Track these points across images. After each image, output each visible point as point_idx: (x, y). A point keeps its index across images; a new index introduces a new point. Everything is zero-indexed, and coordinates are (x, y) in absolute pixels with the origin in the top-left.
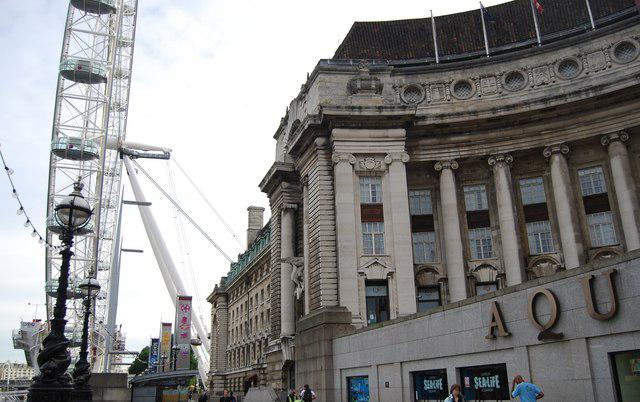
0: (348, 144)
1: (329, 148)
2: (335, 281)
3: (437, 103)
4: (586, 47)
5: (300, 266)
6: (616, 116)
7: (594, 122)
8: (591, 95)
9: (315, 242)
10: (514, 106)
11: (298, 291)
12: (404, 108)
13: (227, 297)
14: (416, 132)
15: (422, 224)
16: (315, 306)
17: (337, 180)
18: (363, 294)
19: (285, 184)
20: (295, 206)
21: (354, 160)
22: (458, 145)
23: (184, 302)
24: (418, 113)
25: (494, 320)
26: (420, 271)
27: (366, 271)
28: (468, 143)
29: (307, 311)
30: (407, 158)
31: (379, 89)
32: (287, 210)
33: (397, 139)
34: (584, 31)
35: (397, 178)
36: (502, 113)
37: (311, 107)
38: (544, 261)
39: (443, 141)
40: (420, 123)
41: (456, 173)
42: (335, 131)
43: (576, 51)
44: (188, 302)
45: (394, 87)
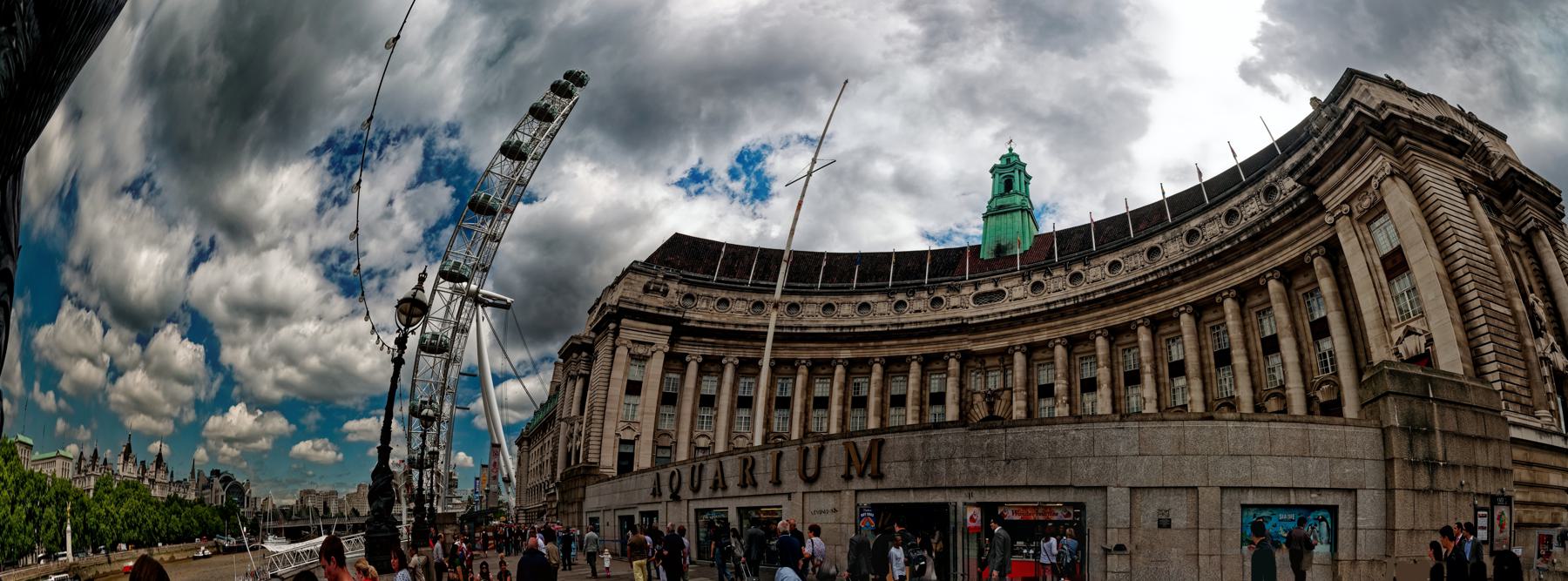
0: (632, 331)
1: (616, 333)
3: (702, 313)
6: (809, 349)
9: (592, 406)
14: (681, 330)
15: (669, 399)
16: (586, 458)
30: (667, 349)
31: (665, 293)
33: (665, 333)
35: (657, 364)
37: (612, 299)
41: (700, 365)
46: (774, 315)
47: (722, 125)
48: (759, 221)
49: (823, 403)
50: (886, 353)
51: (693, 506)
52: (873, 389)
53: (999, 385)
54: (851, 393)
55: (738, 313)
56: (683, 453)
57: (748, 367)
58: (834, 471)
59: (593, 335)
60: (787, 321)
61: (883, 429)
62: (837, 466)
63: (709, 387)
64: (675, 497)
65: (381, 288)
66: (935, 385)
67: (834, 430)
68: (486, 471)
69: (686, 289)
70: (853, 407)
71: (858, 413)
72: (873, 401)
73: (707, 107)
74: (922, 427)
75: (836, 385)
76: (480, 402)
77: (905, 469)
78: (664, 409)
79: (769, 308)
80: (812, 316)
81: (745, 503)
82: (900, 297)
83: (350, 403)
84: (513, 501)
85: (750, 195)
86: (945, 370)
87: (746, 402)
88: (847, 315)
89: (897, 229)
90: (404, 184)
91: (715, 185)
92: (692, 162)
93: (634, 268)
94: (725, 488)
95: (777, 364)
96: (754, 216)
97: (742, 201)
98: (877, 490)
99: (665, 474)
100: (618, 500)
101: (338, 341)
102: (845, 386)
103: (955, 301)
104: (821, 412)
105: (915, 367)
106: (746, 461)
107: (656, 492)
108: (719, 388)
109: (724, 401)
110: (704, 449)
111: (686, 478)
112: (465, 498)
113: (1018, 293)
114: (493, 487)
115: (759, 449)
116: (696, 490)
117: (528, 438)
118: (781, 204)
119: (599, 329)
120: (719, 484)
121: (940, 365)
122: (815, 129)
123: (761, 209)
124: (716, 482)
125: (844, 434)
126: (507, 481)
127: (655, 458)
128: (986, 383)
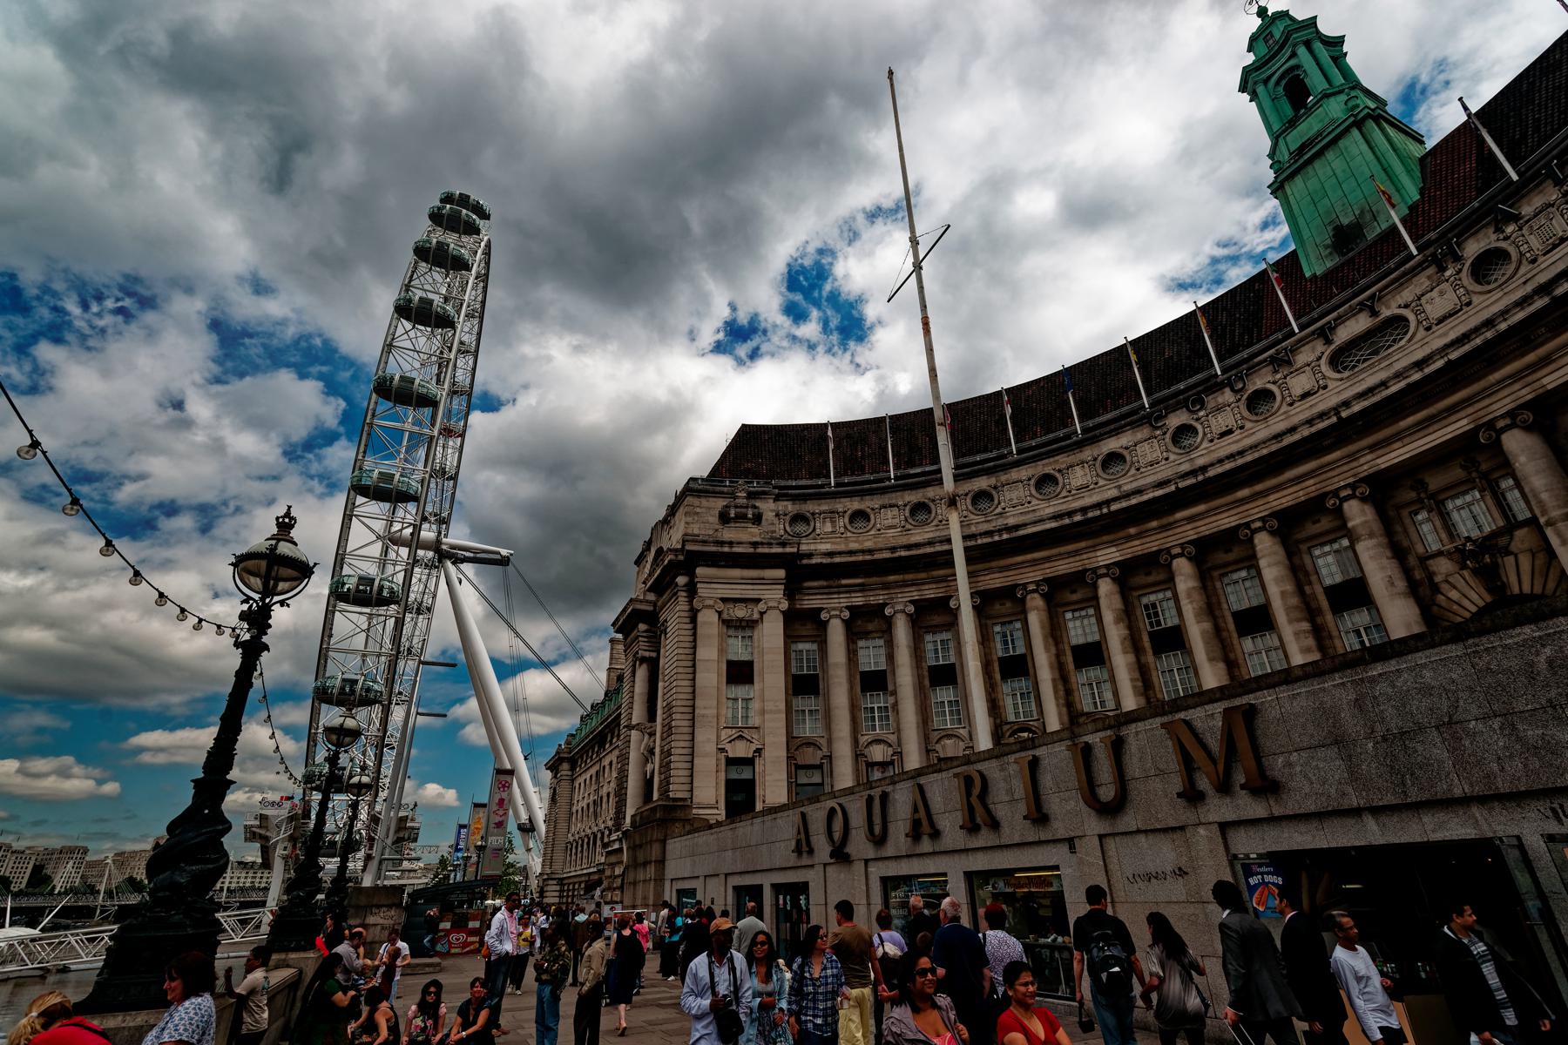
0: (715, 585)
1: (692, 590)
2: (688, 758)
3: (828, 538)
4: (1003, 478)
5: (652, 734)
6: (1035, 562)
7: (1007, 568)
8: (1005, 536)
9: (669, 708)
10: (917, 545)
11: (649, 767)
12: (783, 544)
13: (573, 764)
14: (799, 573)
15: (804, 685)
16: (665, 791)
17: (699, 631)
18: (722, 776)
19: (642, 627)
20: (654, 655)
21: (720, 607)
22: (850, 589)
23: (503, 778)
24: (803, 547)
25: (916, 810)
26: (795, 744)
27: (728, 747)
28: (863, 588)
29: (656, 796)
30: (785, 605)
31: (758, 519)
32: (643, 660)
33: (775, 582)
34: (1004, 456)
35: (772, 632)
36: (903, 553)
38: (949, 736)
39: (831, 583)
40: (805, 561)
41: (848, 624)
42: (700, 571)
43: (993, 481)
44: (507, 778)
45: (777, 515)
46: (954, 518)
47: (735, 238)
48: (869, 375)
49: (1092, 654)
50: (1190, 533)
51: (877, 871)
52: (1189, 610)
53: (1490, 523)
54: (1145, 626)
55: (889, 528)
56: (844, 775)
57: (934, 615)
58: (1156, 785)
59: (651, 597)
60: (979, 524)
61: (1238, 684)
62: (1161, 773)
63: (871, 656)
64: (840, 855)
65: (205, 530)
66: (1329, 568)
67: (1130, 702)
68: (482, 813)
69: (790, 507)
70: (1157, 652)
71: (1173, 661)
72: (1196, 632)
73: (695, 214)
74: (1330, 663)
75: (1108, 617)
76: (473, 704)
77: (1330, 766)
78: (800, 703)
79: (941, 510)
80: (1020, 504)
81: (980, 863)
82: (1176, 420)
83: (150, 703)
84: (536, 864)
85: (835, 338)
86: (1342, 528)
87: (946, 675)
88: (1084, 484)
89: (1111, 298)
90: (197, 378)
91: (775, 339)
92: (722, 312)
93: (692, 489)
94: (936, 834)
95: (984, 602)
96: (859, 369)
97: (829, 351)
98: (1272, 820)
99: (817, 814)
100: (729, 861)
101: (107, 605)
102: (1127, 615)
103: (1299, 384)
104: (1094, 673)
105: (1265, 544)
106: (968, 781)
107: (804, 846)
108: (891, 657)
109: (905, 677)
110: (883, 765)
111: (858, 819)
112: (434, 859)
113: (1437, 305)
114: (495, 841)
115: (988, 756)
116: (879, 840)
117: (568, 761)
118: (895, 338)
119: (661, 586)
120: (923, 827)
121: (1325, 524)
122: (886, 188)
123: (864, 355)
124: (916, 824)
125: (1153, 706)
126: (528, 829)
127: (794, 786)
128: (1449, 528)
